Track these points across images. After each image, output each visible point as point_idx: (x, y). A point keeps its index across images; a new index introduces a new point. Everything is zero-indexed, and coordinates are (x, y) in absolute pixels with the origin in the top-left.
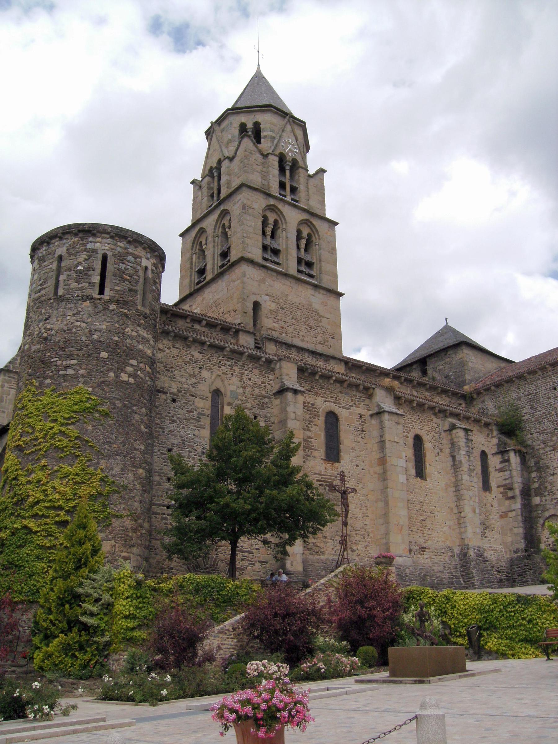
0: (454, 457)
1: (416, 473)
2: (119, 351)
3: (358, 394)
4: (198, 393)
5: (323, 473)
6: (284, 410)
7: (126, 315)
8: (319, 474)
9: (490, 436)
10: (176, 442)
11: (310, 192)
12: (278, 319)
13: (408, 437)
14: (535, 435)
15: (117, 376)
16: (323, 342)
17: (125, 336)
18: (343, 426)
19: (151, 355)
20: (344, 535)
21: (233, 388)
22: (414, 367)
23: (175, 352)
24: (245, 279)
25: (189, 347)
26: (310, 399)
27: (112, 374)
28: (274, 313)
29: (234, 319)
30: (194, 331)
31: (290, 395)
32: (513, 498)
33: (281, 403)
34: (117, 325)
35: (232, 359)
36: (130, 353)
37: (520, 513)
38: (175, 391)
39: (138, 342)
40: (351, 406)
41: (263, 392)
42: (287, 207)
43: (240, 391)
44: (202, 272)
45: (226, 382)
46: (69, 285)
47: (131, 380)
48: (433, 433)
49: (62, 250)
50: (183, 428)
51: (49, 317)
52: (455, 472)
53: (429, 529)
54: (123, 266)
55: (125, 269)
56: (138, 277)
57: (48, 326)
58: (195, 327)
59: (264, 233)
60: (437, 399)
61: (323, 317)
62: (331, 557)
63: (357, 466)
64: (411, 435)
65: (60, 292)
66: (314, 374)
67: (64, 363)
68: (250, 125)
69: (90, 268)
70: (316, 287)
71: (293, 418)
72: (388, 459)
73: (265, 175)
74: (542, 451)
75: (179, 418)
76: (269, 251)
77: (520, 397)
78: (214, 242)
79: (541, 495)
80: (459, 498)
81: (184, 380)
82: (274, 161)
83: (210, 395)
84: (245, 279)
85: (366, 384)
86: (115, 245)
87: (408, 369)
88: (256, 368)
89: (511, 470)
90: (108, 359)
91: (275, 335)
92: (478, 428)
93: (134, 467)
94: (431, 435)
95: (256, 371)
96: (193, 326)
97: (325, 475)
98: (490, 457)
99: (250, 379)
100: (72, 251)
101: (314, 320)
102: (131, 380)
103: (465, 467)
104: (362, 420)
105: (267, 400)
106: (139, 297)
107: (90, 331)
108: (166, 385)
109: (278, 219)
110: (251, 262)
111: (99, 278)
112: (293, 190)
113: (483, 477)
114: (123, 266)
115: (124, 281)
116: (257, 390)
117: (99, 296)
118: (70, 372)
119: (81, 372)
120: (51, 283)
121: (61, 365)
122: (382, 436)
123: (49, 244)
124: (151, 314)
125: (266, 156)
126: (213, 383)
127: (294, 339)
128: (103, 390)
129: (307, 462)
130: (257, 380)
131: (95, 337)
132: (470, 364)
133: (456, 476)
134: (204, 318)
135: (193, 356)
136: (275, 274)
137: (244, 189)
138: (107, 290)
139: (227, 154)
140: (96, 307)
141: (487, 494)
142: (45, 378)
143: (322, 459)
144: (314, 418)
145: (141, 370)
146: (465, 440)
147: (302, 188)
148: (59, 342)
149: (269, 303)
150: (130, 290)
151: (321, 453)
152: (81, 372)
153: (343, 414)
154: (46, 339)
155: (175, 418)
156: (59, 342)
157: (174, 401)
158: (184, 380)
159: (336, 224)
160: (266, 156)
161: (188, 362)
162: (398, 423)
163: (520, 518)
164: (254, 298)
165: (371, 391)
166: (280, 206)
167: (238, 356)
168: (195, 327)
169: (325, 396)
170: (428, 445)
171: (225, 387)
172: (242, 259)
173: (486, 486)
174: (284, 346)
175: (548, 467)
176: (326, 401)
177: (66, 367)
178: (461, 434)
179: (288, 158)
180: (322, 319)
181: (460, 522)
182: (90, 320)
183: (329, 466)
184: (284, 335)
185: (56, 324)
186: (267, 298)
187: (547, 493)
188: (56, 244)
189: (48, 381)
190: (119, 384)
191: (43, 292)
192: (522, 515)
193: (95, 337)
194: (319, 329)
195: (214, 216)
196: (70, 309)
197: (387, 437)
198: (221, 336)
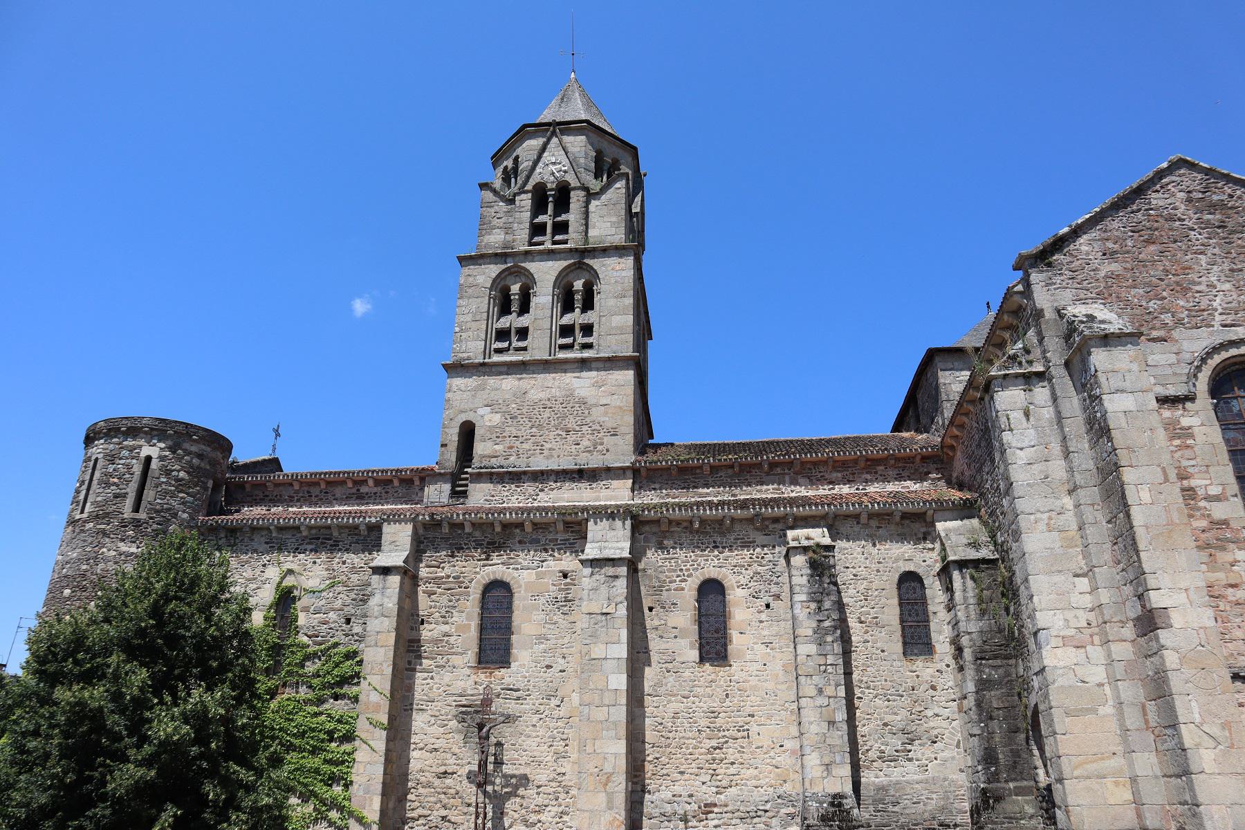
3: (560, 537)
5: (469, 692)
13: (683, 589)
16: (592, 449)
18: (520, 601)
40: (543, 561)
48: (756, 567)
53: (733, 763)
55: (114, 470)
56: (132, 474)
58: (361, 491)
63: (549, 667)
64: (692, 585)
92: (893, 527)
96: (358, 490)
97: (472, 695)
99: (344, 563)
104: (568, 580)
106: (129, 502)
141: (919, 663)
144: (459, 600)
150: (116, 496)
151: (471, 656)
164: (463, 418)
168: (361, 491)
170: (736, 595)
176: (484, 566)
180: (594, 409)
183: (482, 677)
194: (585, 428)
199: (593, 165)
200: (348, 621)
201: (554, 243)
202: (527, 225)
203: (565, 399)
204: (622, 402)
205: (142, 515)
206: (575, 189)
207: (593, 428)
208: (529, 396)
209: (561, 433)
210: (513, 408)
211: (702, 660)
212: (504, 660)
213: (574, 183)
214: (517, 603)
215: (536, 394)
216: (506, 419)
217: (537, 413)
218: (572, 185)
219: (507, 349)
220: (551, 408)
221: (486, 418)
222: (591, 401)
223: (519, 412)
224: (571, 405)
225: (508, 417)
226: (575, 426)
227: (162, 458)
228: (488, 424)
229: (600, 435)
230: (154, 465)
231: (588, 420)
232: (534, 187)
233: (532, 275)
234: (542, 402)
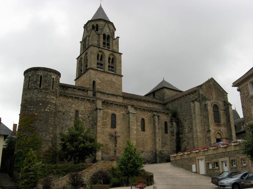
0: (154, 124)
1: (142, 129)
2: (45, 103)
3: (123, 108)
4: (71, 111)
6: (97, 115)
7: (47, 93)
8: (109, 132)
9: (168, 117)
10: (64, 126)
11: (114, 44)
14: (181, 116)
15: (44, 110)
17: (47, 98)
19: (55, 103)
20: (116, 149)
21: (82, 109)
22: (152, 94)
23: (64, 100)
24: (91, 74)
25: (68, 98)
26: (106, 110)
27: (43, 109)
29: (87, 86)
30: (74, 91)
31: (98, 110)
32: (173, 135)
33: (96, 113)
34: (44, 96)
35: (82, 101)
36: (48, 103)
37: (175, 140)
38: (64, 111)
39: (51, 100)
41: (91, 110)
42: (105, 51)
43: (84, 110)
44: (81, 70)
45: (80, 108)
46: (32, 85)
47: (49, 111)
48: (148, 117)
49: (30, 75)
50: (66, 121)
51: (27, 94)
52: (154, 129)
54: (46, 79)
57: (27, 97)
59: (98, 59)
60: (154, 105)
61: (116, 83)
62: (112, 155)
65: (29, 87)
66: (108, 103)
67: (30, 107)
68: (95, 25)
69: (37, 80)
70: (114, 74)
71: (99, 117)
72: (130, 127)
73: (99, 41)
74: (183, 121)
75: (65, 119)
76: (99, 65)
77: (178, 105)
78: (84, 62)
79: (182, 134)
80: (155, 136)
81: (67, 108)
82: (102, 36)
83: (75, 112)
84: (91, 74)
85: (125, 105)
86: (44, 73)
87: (150, 95)
88: (89, 103)
89: (173, 127)
90: (42, 105)
91: (100, 90)
93: (49, 134)
94: (147, 118)
95: (89, 104)
98: (168, 123)
99: (87, 106)
100: (33, 75)
102: (49, 111)
103: (157, 127)
105: (92, 112)
106: (51, 87)
107: (37, 98)
108: (61, 110)
109: (102, 54)
110: (93, 69)
111: (39, 83)
112: (108, 45)
113: (165, 129)
114: (46, 79)
115: (46, 83)
116: (89, 109)
117: (39, 88)
118: (32, 109)
119: (34, 109)
120: (27, 84)
121: (29, 107)
122: (129, 120)
123: (27, 73)
124: (55, 91)
125: (99, 35)
126: (75, 108)
127: (106, 91)
128: (40, 114)
129: (105, 129)
130: (89, 106)
131: (38, 99)
132: (166, 94)
133: (154, 130)
134: (77, 87)
135: (70, 101)
136: (100, 72)
137: (91, 47)
138: (42, 86)
139: (88, 35)
140: (39, 91)
142: (26, 111)
143: (110, 128)
145: (52, 107)
146: (157, 119)
147: (111, 44)
148: (29, 101)
149: (98, 81)
151: (109, 126)
152: (34, 109)
153: (117, 114)
154: (26, 100)
155: (64, 119)
156: (29, 101)
157: (64, 114)
158: (67, 108)
159: (122, 54)
160: (99, 35)
161: (68, 103)
162: (134, 116)
163: (175, 141)
164: (93, 80)
165: (127, 107)
166: (103, 50)
167: (84, 100)
169: (111, 109)
170: (146, 121)
171: (79, 109)
172: (90, 68)
173: (166, 132)
174: (102, 94)
175: (184, 126)
177: (31, 108)
178: (156, 117)
179: (106, 35)
180: (116, 84)
181: (155, 143)
182: (37, 95)
183: (112, 129)
184: (103, 90)
185: (28, 96)
186: (98, 79)
187: (183, 134)
188: (29, 73)
189: (26, 112)
190: (45, 112)
191: (26, 87)
192: (176, 140)
193: (38, 99)
195: (84, 54)
196: (32, 92)
197: (131, 120)
198: (83, 92)
200: (89, 117)
205: (54, 91)
206: (111, 37)
211: (142, 131)
212: (115, 127)
214: (117, 118)
215: (106, 79)
221: (98, 81)
222: (115, 82)
227: (55, 79)
230: (55, 80)
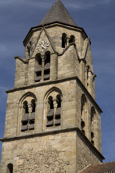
12: (24, 169)
28: (21, 166)
101: (53, 157)
164: (8, 163)
166: (31, 90)
186: (18, 158)
194: (56, 162)
199: (61, 41)
201: (45, 79)
202: (33, 73)
203: (48, 150)
204: (71, 149)
207: (59, 162)
208: (34, 150)
209: (46, 165)
210: (28, 156)
213: (52, 51)
216: (25, 161)
217: (37, 157)
218: (51, 53)
219: (26, 130)
220: (43, 154)
221: (17, 162)
222: (59, 150)
223: (30, 158)
224: (51, 152)
225: (26, 160)
226: (52, 162)
228: (18, 164)
229: (62, 165)
231: (57, 159)
232: (36, 55)
233: (35, 96)
234: (40, 152)
